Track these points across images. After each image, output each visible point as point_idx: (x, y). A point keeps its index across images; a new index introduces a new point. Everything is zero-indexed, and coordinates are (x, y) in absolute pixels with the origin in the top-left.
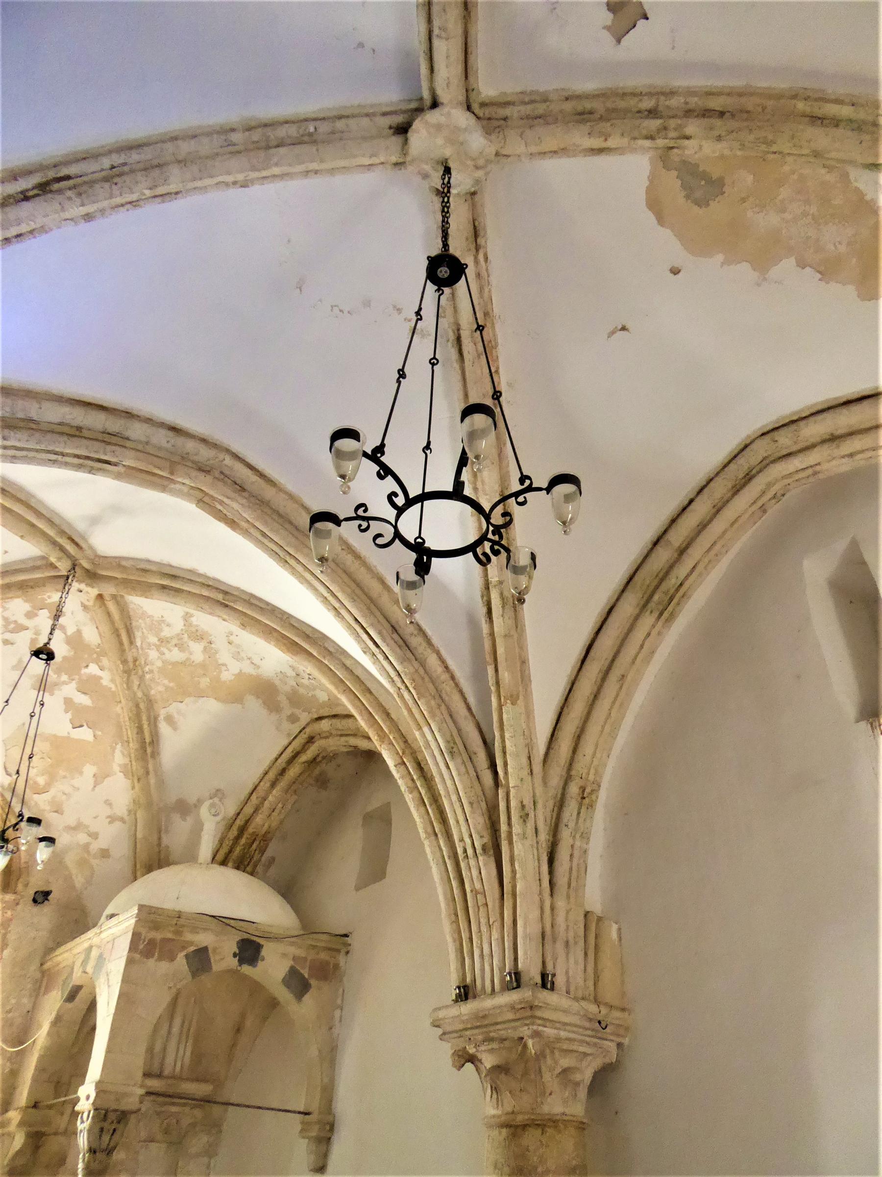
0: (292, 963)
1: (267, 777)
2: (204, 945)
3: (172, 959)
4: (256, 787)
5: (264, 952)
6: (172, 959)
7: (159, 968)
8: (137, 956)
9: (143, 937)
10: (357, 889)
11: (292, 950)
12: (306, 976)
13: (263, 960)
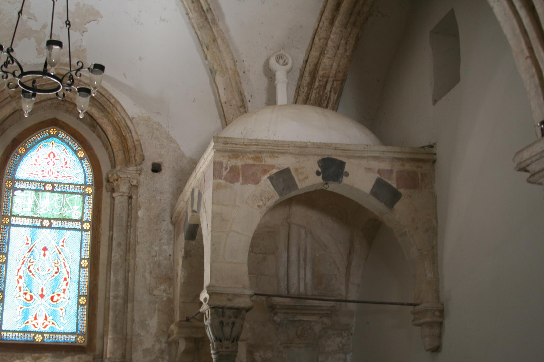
0: (378, 176)
1: (323, 18)
2: (285, 167)
3: (256, 182)
4: (317, 30)
5: (347, 168)
6: (256, 182)
7: (244, 191)
8: (222, 182)
9: (224, 165)
10: (435, 102)
11: (376, 165)
12: (395, 186)
13: (347, 175)
